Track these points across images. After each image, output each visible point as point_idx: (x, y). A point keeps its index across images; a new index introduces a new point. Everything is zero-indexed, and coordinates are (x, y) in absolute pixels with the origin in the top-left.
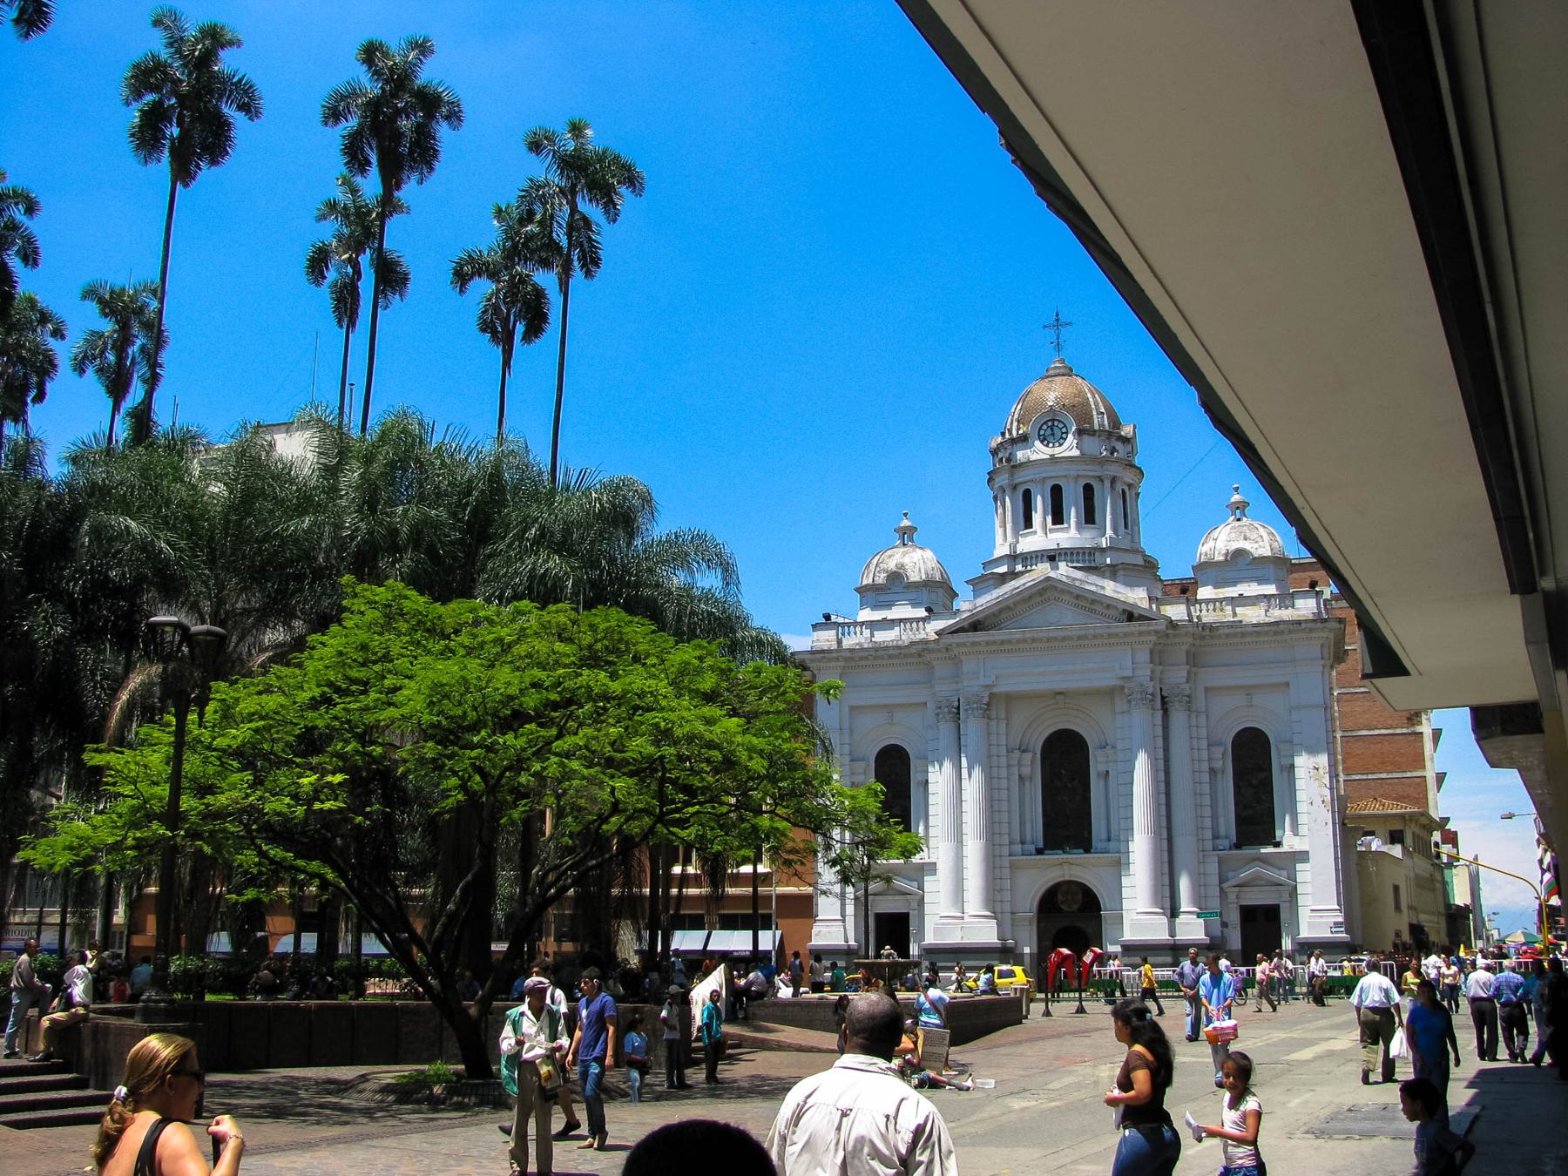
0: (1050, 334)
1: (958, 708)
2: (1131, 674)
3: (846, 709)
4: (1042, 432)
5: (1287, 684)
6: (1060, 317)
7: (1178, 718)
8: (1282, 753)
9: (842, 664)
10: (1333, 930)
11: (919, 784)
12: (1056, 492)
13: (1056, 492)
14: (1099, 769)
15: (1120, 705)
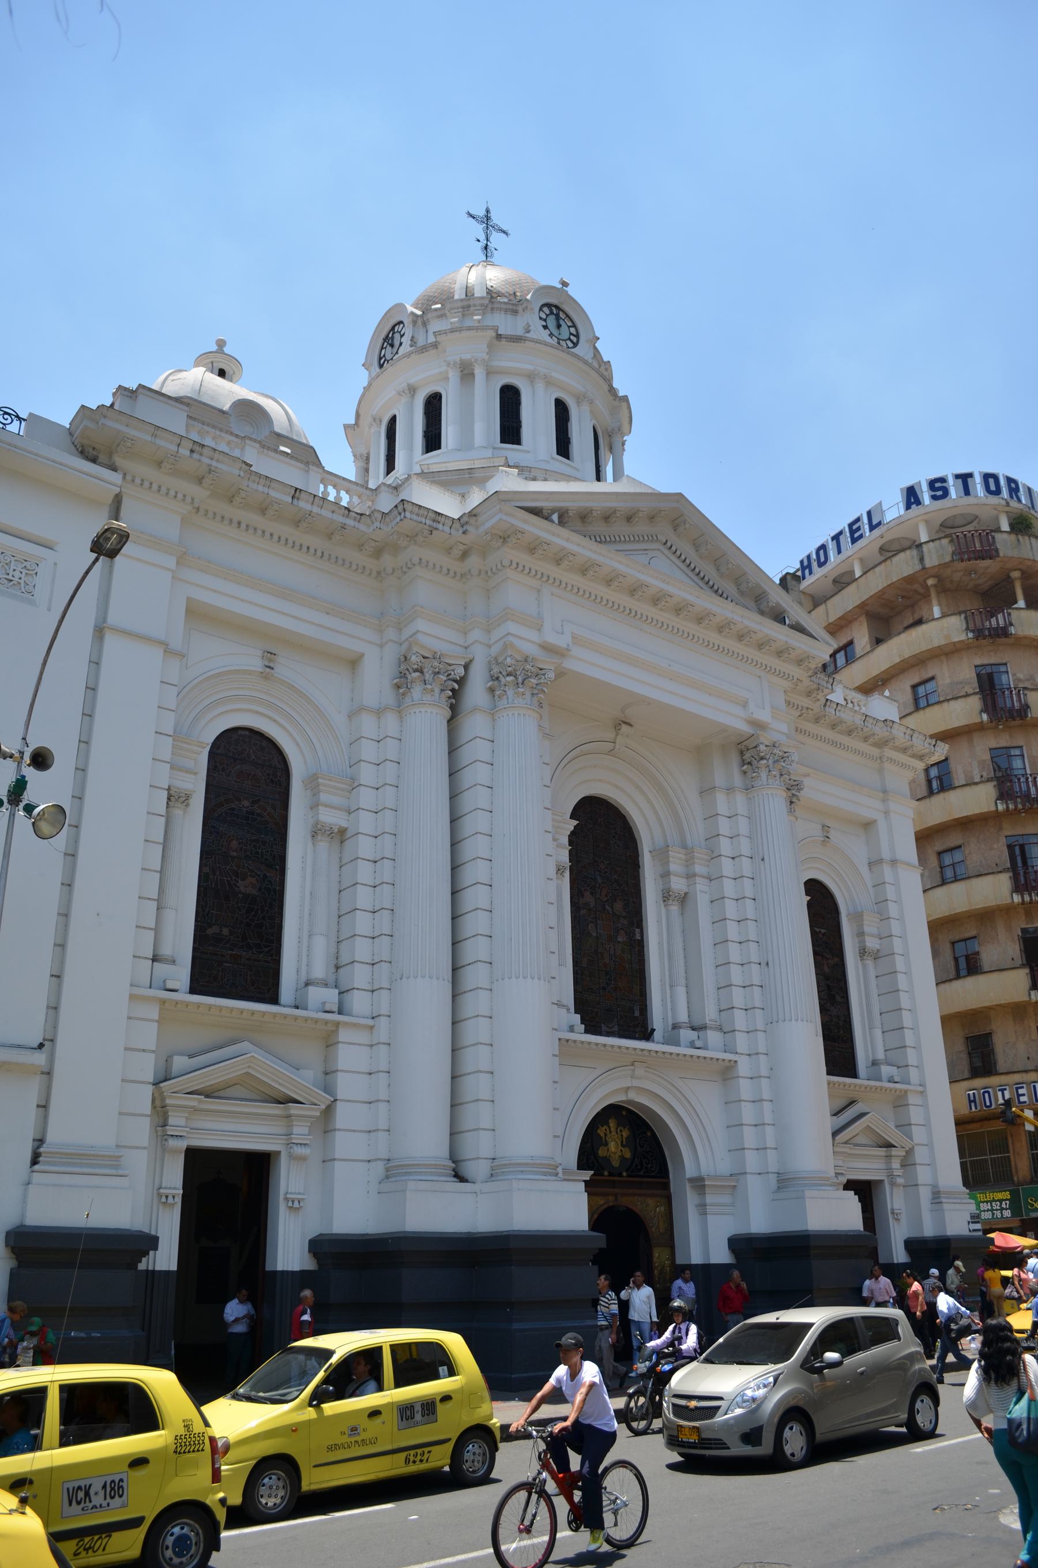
6: (492, 215)
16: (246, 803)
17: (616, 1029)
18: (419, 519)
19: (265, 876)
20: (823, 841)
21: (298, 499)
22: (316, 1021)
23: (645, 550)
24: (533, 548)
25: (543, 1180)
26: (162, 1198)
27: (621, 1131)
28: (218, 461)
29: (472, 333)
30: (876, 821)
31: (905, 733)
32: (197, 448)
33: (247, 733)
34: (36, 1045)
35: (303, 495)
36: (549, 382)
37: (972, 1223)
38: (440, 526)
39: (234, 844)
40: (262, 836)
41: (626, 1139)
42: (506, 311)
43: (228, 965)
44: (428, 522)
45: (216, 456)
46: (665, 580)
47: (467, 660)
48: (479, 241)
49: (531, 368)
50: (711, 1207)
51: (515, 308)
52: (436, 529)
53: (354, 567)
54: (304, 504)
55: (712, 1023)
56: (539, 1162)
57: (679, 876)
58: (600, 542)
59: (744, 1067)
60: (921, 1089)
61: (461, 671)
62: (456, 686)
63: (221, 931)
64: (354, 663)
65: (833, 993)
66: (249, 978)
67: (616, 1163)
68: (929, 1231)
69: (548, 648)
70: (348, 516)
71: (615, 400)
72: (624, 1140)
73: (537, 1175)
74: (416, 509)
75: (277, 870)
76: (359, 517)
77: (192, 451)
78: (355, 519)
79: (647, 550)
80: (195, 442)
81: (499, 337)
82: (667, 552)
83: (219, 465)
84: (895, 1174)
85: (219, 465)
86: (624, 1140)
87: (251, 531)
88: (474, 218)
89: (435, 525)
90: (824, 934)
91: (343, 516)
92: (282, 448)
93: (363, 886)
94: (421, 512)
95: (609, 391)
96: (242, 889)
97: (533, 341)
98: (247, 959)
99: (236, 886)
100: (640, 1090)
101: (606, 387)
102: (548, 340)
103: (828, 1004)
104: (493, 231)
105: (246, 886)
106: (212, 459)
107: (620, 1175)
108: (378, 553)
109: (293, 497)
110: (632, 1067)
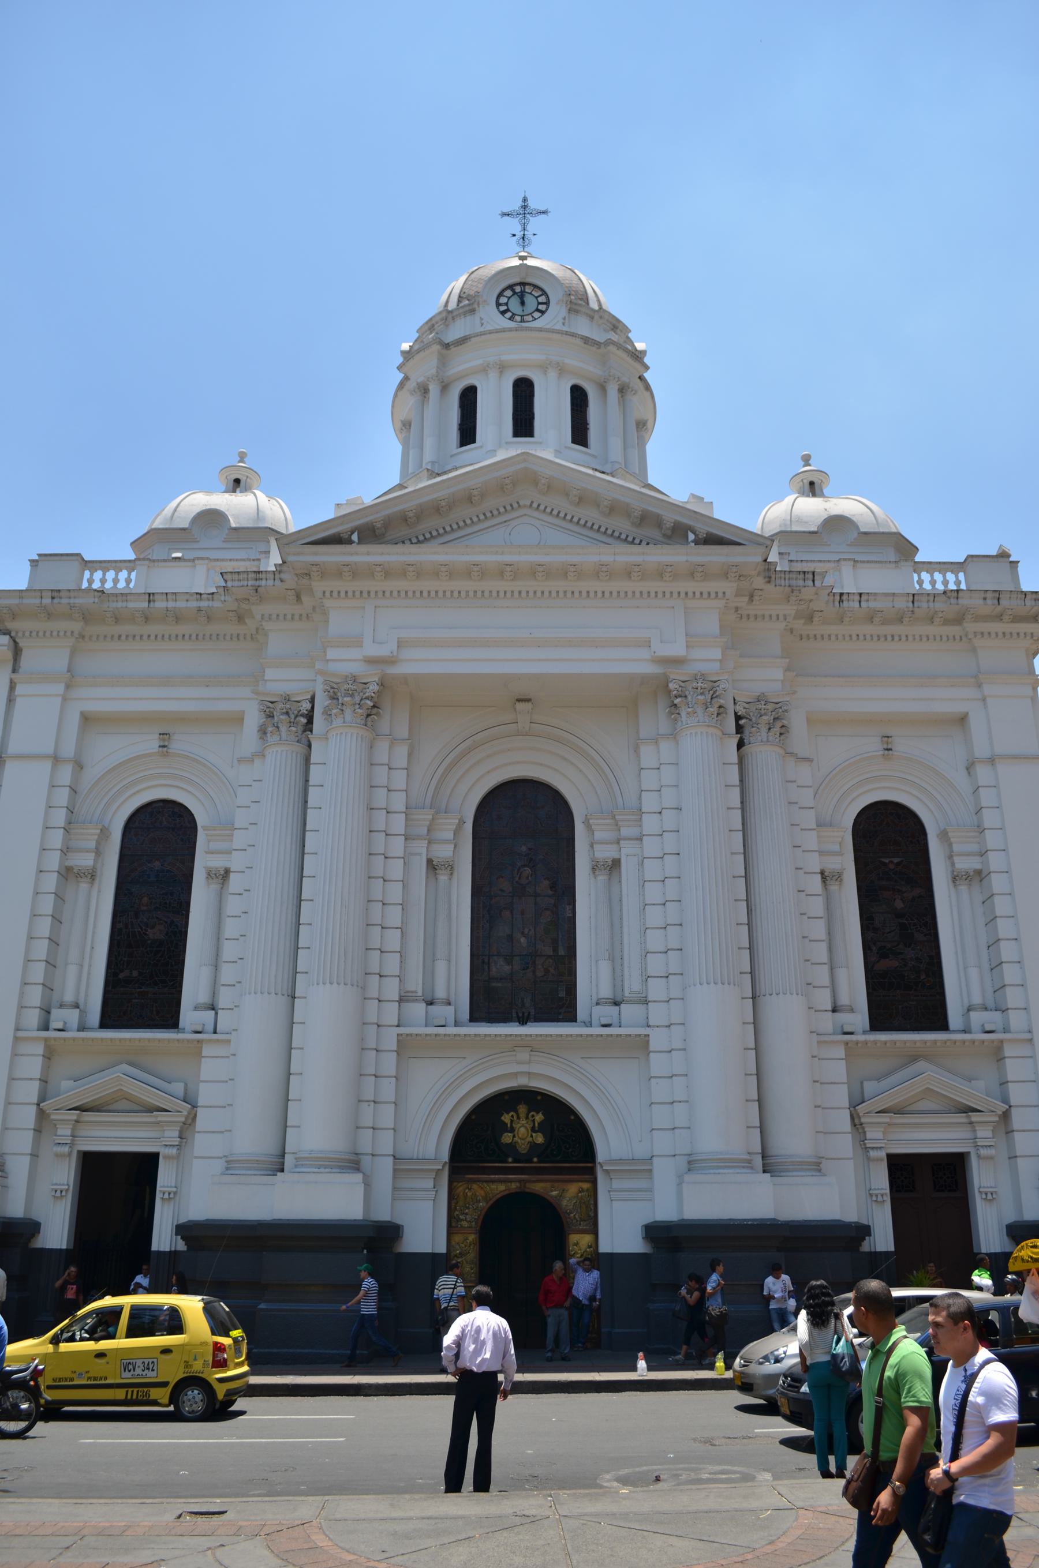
0: (514, 225)
2: (677, 649)
3: (74, 721)
4: (503, 300)
8: (956, 848)
9: (77, 626)
11: (210, 874)
12: (523, 391)
13: (523, 391)
16: (157, 864)
18: (241, 583)
19: (172, 922)
20: (883, 755)
21: (154, 601)
22: (193, 1041)
23: (505, 522)
24: (339, 572)
25: (314, 1173)
26: (58, 1195)
27: (533, 1116)
28: (75, 598)
29: (422, 354)
31: (985, 599)
32: (55, 594)
33: (161, 804)
35: (156, 597)
36: (502, 368)
38: (263, 583)
39: (145, 900)
40: (171, 888)
41: (539, 1124)
42: (465, 314)
43: (137, 1001)
44: (250, 583)
45: (72, 594)
46: (497, 552)
47: (311, 693)
48: (514, 235)
49: (479, 362)
50: (614, 1193)
51: (471, 308)
52: (259, 586)
53: (228, 637)
54: (160, 604)
55: (634, 995)
56: (316, 1155)
57: (611, 843)
58: (419, 542)
59: (658, 1040)
60: (1027, 1036)
65: (909, 931)
66: (154, 1009)
67: (523, 1148)
69: (371, 661)
70: (201, 599)
71: (599, 348)
72: (536, 1125)
73: (250, 1170)
74: (236, 576)
75: (183, 914)
76: (211, 596)
77: (53, 598)
78: (208, 600)
79: (509, 520)
80: (52, 590)
81: (447, 346)
82: (536, 514)
83: (77, 601)
84: (979, 1144)
85: (77, 601)
86: (536, 1125)
87: (130, 639)
88: (508, 215)
89: (258, 583)
90: (898, 864)
91: (197, 600)
92: (174, 555)
93: (231, 918)
94: (241, 576)
95: (585, 343)
97: (478, 336)
99: (146, 934)
101: (578, 341)
102: (511, 324)
104: (530, 218)
105: (156, 933)
106: (70, 598)
107: (532, 1162)
108: (240, 619)
109: (149, 601)
110: (514, 1053)
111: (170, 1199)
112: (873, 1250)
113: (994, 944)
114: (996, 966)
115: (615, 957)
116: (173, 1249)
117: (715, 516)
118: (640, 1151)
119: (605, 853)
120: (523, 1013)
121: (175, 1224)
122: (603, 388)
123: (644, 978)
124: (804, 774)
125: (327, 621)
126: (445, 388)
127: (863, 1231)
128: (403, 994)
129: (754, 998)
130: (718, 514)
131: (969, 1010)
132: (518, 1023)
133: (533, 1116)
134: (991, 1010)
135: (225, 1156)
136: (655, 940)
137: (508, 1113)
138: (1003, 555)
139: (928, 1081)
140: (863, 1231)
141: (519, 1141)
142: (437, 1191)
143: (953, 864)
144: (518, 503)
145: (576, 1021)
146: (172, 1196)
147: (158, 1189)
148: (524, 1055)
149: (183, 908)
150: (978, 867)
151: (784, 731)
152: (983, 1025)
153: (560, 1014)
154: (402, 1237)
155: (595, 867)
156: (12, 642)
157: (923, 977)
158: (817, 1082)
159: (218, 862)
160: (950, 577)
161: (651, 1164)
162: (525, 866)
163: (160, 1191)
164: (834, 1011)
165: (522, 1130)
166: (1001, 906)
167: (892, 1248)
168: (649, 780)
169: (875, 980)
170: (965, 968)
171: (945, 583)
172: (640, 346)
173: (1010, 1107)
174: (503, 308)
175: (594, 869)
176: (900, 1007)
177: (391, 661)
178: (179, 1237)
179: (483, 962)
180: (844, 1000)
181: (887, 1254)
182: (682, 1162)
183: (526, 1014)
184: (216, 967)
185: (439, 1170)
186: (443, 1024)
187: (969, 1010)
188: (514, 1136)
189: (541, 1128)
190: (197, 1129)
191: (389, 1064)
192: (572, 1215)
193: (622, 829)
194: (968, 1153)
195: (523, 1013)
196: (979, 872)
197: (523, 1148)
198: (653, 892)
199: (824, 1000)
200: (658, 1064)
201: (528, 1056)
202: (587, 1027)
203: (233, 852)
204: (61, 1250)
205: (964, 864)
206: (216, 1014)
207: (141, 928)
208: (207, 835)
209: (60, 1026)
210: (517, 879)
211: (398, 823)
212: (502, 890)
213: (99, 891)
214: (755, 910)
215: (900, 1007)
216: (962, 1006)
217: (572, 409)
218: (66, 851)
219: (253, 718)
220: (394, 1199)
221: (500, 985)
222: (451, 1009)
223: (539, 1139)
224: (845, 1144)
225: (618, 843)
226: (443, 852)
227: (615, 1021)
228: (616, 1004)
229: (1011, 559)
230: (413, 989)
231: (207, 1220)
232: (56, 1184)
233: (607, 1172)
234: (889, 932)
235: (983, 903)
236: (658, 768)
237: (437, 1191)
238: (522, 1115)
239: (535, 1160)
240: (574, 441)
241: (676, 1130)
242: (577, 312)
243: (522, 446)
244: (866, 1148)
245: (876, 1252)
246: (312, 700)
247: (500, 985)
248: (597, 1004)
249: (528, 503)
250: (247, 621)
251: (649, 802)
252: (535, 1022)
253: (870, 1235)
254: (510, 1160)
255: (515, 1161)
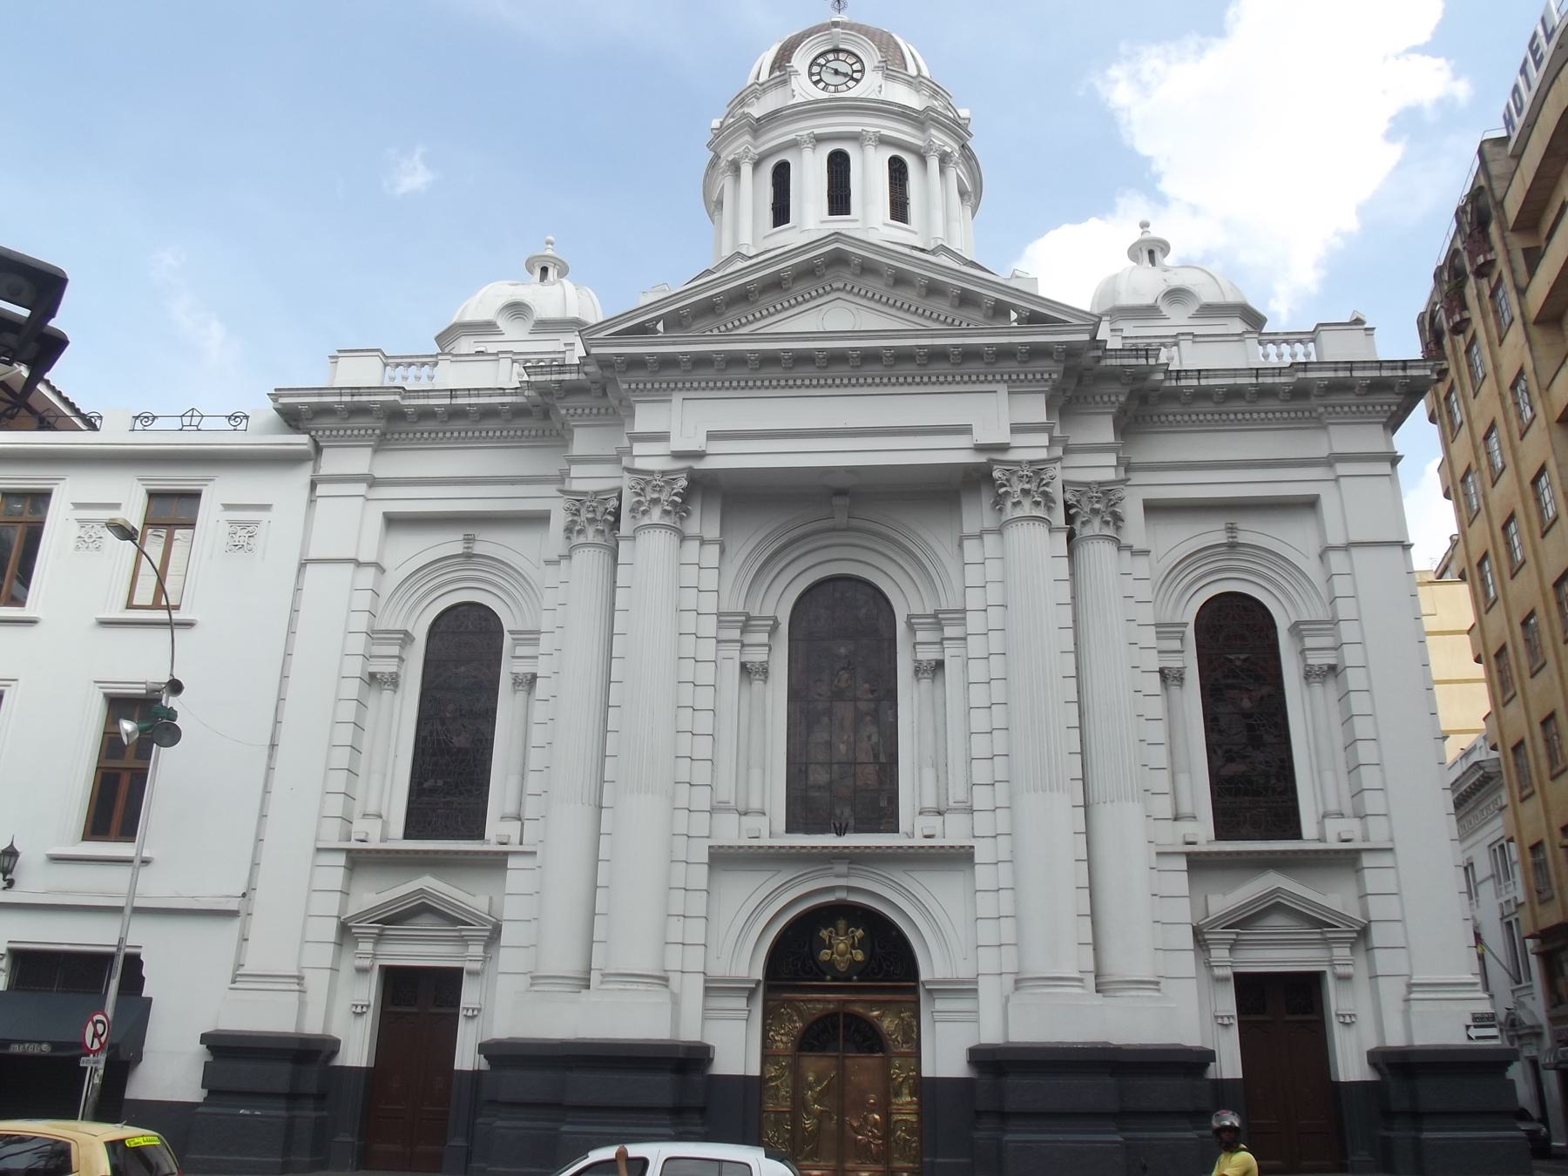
1: (617, 514)
2: (1002, 436)
3: (378, 521)
4: (816, 69)
5: (1310, 504)
7: (1099, 556)
10: (1474, 1032)
11: (517, 681)
12: (839, 166)
13: (839, 166)
14: (920, 657)
15: (977, 515)
17: (852, 823)
22: (497, 853)
30: (1318, 495)
34: (240, 895)
37: (1475, 1027)
39: (451, 707)
41: (859, 940)
42: (776, 85)
43: (443, 811)
61: (615, 503)
62: (611, 518)
63: (436, 782)
64: (539, 519)
65: (1258, 733)
67: (842, 967)
68: (1396, 1038)
69: (677, 455)
90: (1245, 660)
96: (457, 745)
98: (459, 804)
100: (850, 889)
103: (1250, 748)
105: (459, 741)
107: (850, 979)
111: (473, 1017)
112: (1219, 1077)
113: (1351, 744)
114: (1354, 768)
115: (940, 766)
116: (476, 1068)
117: (1042, 293)
118: (964, 972)
119: (928, 654)
120: (841, 825)
121: (479, 1042)
122: (923, 159)
123: (969, 785)
124: (1141, 566)
125: (633, 416)
126: (757, 165)
127: (1205, 1057)
128: (715, 804)
129: (1086, 806)
130: (1044, 291)
131: (1325, 816)
132: (835, 835)
133: (852, 932)
134: (1349, 817)
135: (530, 972)
136: (980, 746)
137: (826, 928)
138: (1358, 322)
139: (1279, 894)
140: (1205, 1057)
141: (838, 958)
142: (750, 1011)
143: (1305, 659)
144: (831, 286)
145: (898, 832)
146: (476, 1013)
147: (462, 1005)
148: (842, 868)
149: (490, 715)
150: (1332, 661)
151: (1117, 519)
152: (1339, 834)
153: (881, 824)
154: (712, 1059)
155: (918, 670)
156: (311, 440)
157: (1273, 781)
158: (1156, 895)
159: (523, 668)
160: (1299, 347)
161: (977, 983)
162: (843, 669)
163: (464, 1008)
164: (1176, 819)
165: (842, 946)
166: (1358, 703)
167: (1240, 1076)
168: (973, 575)
169: (1221, 787)
170: (1319, 772)
171: (1293, 355)
172: (964, 113)
173: (1370, 922)
174: (815, 78)
175: (917, 671)
176: (1248, 814)
177: (700, 455)
178: (483, 1056)
179: (800, 770)
180: (1186, 808)
181: (1232, 1082)
182: (1009, 981)
183: (843, 825)
184: (523, 777)
185: (753, 988)
186: (757, 835)
187: (1325, 816)
188: (832, 954)
189: (861, 945)
190: (502, 944)
191: (700, 875)
192: (894, 1037)
193: (945, 628)
194: (1324, 972)
195: (841, 825)
196: (1332, 668)
197: (842, 967)
198: (978, 696)
199: (1164, 807)
200: (983, 875)
201: (846, 869)
202: (909, 837)
203: (540, 657)
204: (361, 1068)
205: (1317, 660)
206: (523, 824)
207: (446, 736)
208: (513, 639)
209: (362, 837)
210: (836, 682)
211: (709, 626)
212: (820, 695)
213: (403, 698)
214: (1088, 713)
215: (1248, 814)
216: (1317, 811)
217: (891, 183)
218: (367, 657)
219: (559, 520)
220: (705, 1019)
221: (817, 794)
222: (765, 820)
223: (859, 956)
224: (1187, 962)
225: (941, 643)
226: (757, 656)
227: (938, 831)
228: (940, 813)
229: (1366, 326)
230: (726, 799)
231: (510, 1038)
232: (358, 1000)
233: (930, 991)
234: (1235, 735)
235: (1339, 700)
236: (983, 563)
237: (750, 1011)
238: (842, 931)
239: (855, 978)
240: (893, 218)
241: (1003, 947)
242: (894, 78)
243: (840, 224)
244: (1211, 966)
245: (1222, 1080)
246: (620, 498)
247: (817, 794)
248: (921, 813)
249: (842, 286)
250: (552, 416)
251: (974, 600)
252: (855, 832)
253: (1215, 1061)
254: (828, 977)
255: (834, 979)
